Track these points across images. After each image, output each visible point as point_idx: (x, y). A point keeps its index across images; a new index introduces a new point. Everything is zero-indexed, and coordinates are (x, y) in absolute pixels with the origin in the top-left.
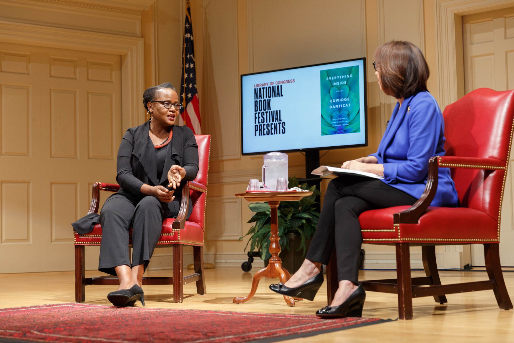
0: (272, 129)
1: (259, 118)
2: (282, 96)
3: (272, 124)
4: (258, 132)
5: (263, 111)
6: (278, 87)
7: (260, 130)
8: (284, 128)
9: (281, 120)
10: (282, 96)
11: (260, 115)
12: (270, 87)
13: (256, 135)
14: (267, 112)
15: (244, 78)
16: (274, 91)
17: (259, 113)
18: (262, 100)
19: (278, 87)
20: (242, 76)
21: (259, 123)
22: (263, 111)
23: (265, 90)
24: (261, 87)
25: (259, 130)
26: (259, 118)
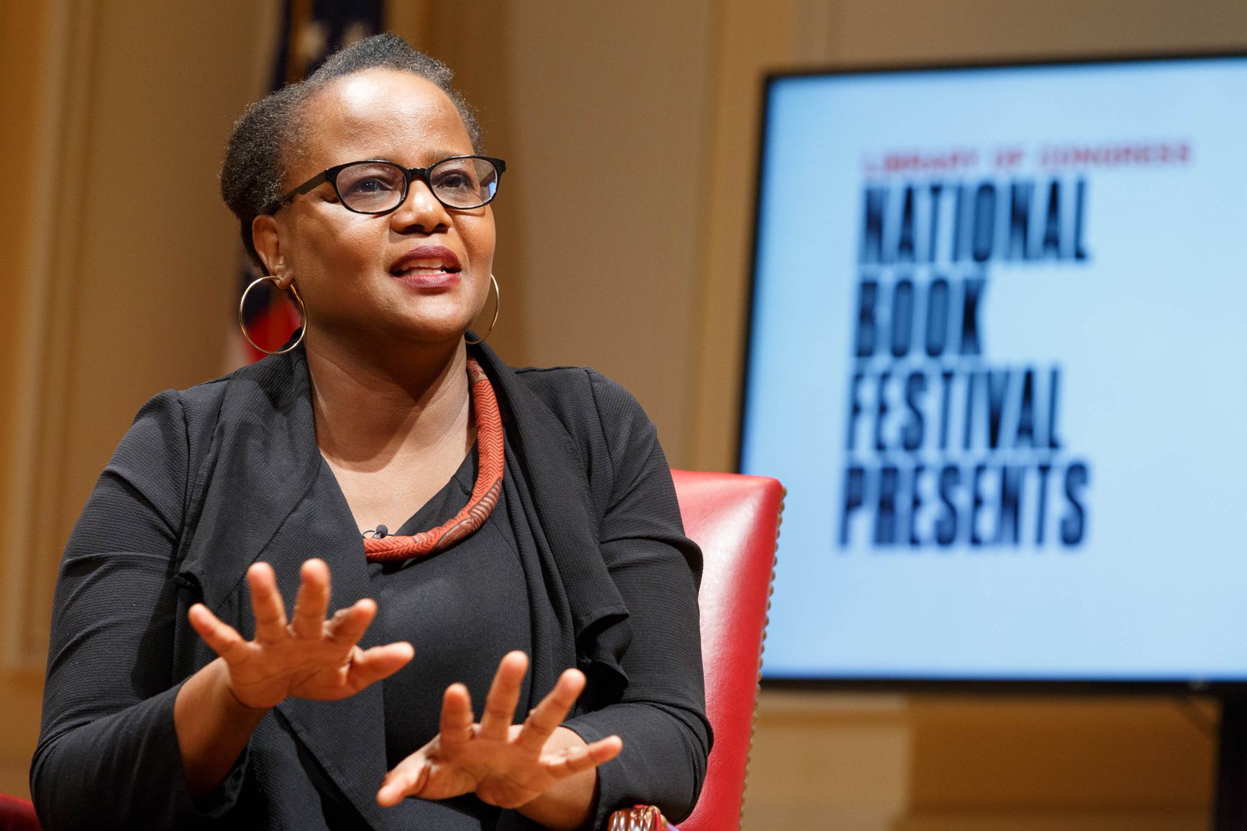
0: (978, 502)
1: (883, 409)
2: (1080, 255)
3: (980, 469)
4: (864, 522)
5: (917, 359)
6: (1055, 190)
7: (886, 506)
8: (1079, 510)
9: (1053, 444)
10: (1080, 255)
11: (895, 392)
12: (987, 189)
13: (844, 537)
14: (948, 376)
15: (793, 103)
16: (1019, 218)
17: (885, 377)
18: (922, 275)
19: (1055, 190)
20: (770, 81)
21: (880, 446)
22: (917, 359)
23: (947, 204)
24: (922, 178)
25: (878, 500)
26: (883, 409)
